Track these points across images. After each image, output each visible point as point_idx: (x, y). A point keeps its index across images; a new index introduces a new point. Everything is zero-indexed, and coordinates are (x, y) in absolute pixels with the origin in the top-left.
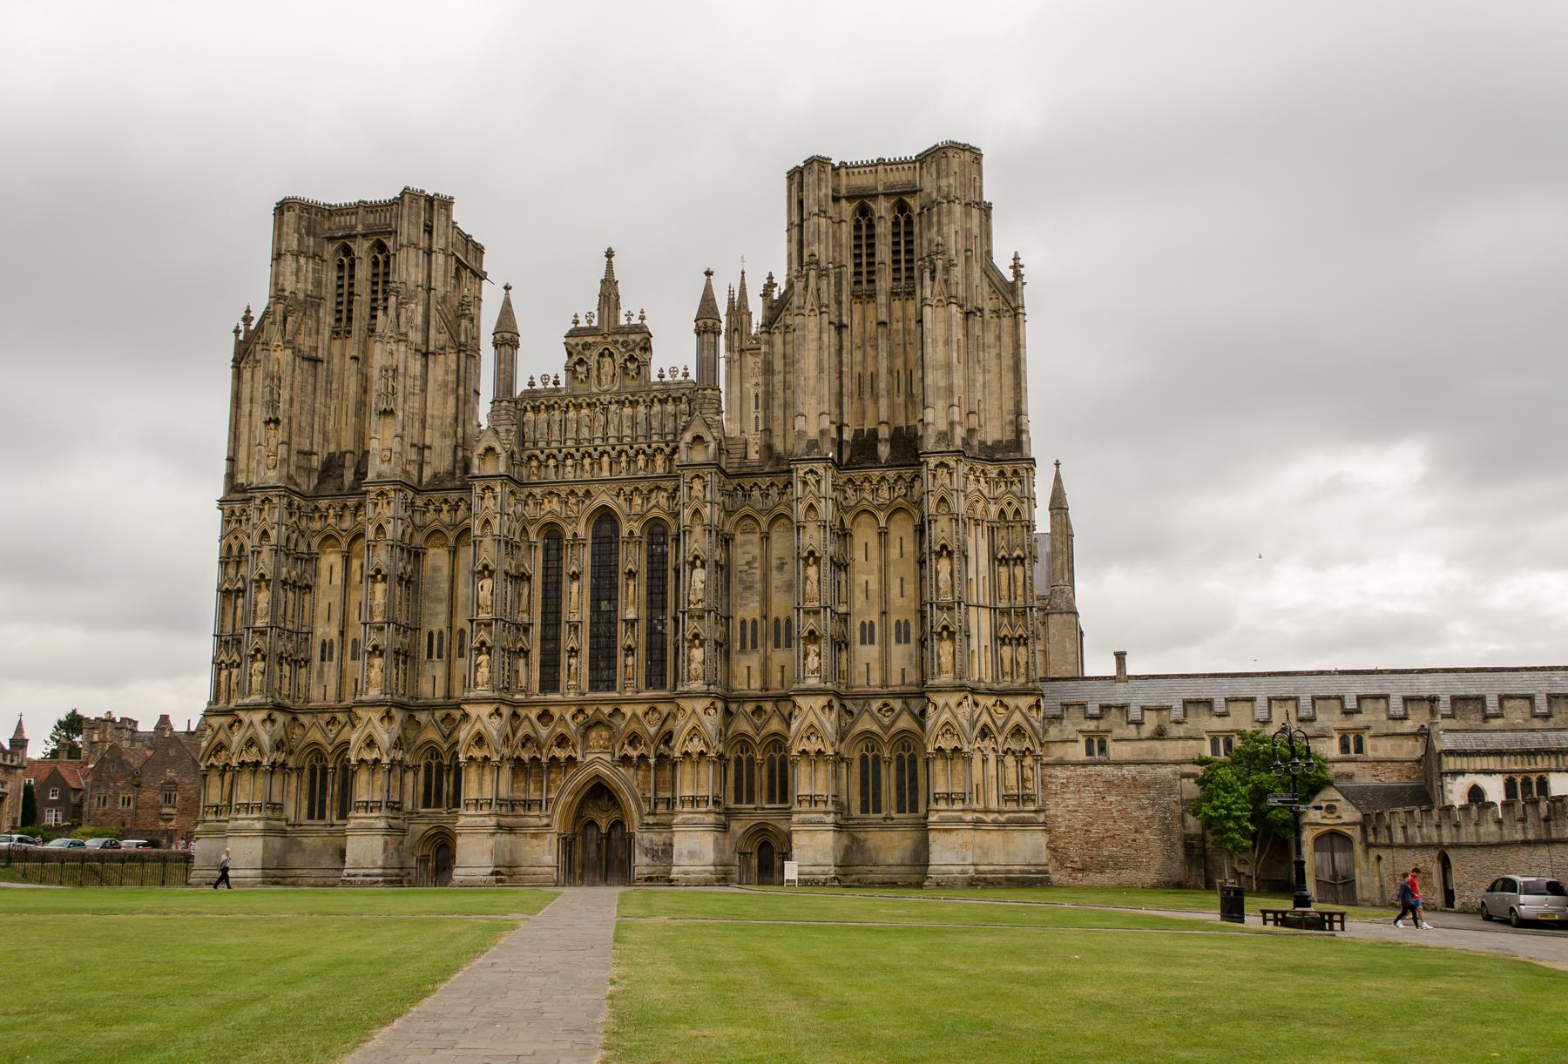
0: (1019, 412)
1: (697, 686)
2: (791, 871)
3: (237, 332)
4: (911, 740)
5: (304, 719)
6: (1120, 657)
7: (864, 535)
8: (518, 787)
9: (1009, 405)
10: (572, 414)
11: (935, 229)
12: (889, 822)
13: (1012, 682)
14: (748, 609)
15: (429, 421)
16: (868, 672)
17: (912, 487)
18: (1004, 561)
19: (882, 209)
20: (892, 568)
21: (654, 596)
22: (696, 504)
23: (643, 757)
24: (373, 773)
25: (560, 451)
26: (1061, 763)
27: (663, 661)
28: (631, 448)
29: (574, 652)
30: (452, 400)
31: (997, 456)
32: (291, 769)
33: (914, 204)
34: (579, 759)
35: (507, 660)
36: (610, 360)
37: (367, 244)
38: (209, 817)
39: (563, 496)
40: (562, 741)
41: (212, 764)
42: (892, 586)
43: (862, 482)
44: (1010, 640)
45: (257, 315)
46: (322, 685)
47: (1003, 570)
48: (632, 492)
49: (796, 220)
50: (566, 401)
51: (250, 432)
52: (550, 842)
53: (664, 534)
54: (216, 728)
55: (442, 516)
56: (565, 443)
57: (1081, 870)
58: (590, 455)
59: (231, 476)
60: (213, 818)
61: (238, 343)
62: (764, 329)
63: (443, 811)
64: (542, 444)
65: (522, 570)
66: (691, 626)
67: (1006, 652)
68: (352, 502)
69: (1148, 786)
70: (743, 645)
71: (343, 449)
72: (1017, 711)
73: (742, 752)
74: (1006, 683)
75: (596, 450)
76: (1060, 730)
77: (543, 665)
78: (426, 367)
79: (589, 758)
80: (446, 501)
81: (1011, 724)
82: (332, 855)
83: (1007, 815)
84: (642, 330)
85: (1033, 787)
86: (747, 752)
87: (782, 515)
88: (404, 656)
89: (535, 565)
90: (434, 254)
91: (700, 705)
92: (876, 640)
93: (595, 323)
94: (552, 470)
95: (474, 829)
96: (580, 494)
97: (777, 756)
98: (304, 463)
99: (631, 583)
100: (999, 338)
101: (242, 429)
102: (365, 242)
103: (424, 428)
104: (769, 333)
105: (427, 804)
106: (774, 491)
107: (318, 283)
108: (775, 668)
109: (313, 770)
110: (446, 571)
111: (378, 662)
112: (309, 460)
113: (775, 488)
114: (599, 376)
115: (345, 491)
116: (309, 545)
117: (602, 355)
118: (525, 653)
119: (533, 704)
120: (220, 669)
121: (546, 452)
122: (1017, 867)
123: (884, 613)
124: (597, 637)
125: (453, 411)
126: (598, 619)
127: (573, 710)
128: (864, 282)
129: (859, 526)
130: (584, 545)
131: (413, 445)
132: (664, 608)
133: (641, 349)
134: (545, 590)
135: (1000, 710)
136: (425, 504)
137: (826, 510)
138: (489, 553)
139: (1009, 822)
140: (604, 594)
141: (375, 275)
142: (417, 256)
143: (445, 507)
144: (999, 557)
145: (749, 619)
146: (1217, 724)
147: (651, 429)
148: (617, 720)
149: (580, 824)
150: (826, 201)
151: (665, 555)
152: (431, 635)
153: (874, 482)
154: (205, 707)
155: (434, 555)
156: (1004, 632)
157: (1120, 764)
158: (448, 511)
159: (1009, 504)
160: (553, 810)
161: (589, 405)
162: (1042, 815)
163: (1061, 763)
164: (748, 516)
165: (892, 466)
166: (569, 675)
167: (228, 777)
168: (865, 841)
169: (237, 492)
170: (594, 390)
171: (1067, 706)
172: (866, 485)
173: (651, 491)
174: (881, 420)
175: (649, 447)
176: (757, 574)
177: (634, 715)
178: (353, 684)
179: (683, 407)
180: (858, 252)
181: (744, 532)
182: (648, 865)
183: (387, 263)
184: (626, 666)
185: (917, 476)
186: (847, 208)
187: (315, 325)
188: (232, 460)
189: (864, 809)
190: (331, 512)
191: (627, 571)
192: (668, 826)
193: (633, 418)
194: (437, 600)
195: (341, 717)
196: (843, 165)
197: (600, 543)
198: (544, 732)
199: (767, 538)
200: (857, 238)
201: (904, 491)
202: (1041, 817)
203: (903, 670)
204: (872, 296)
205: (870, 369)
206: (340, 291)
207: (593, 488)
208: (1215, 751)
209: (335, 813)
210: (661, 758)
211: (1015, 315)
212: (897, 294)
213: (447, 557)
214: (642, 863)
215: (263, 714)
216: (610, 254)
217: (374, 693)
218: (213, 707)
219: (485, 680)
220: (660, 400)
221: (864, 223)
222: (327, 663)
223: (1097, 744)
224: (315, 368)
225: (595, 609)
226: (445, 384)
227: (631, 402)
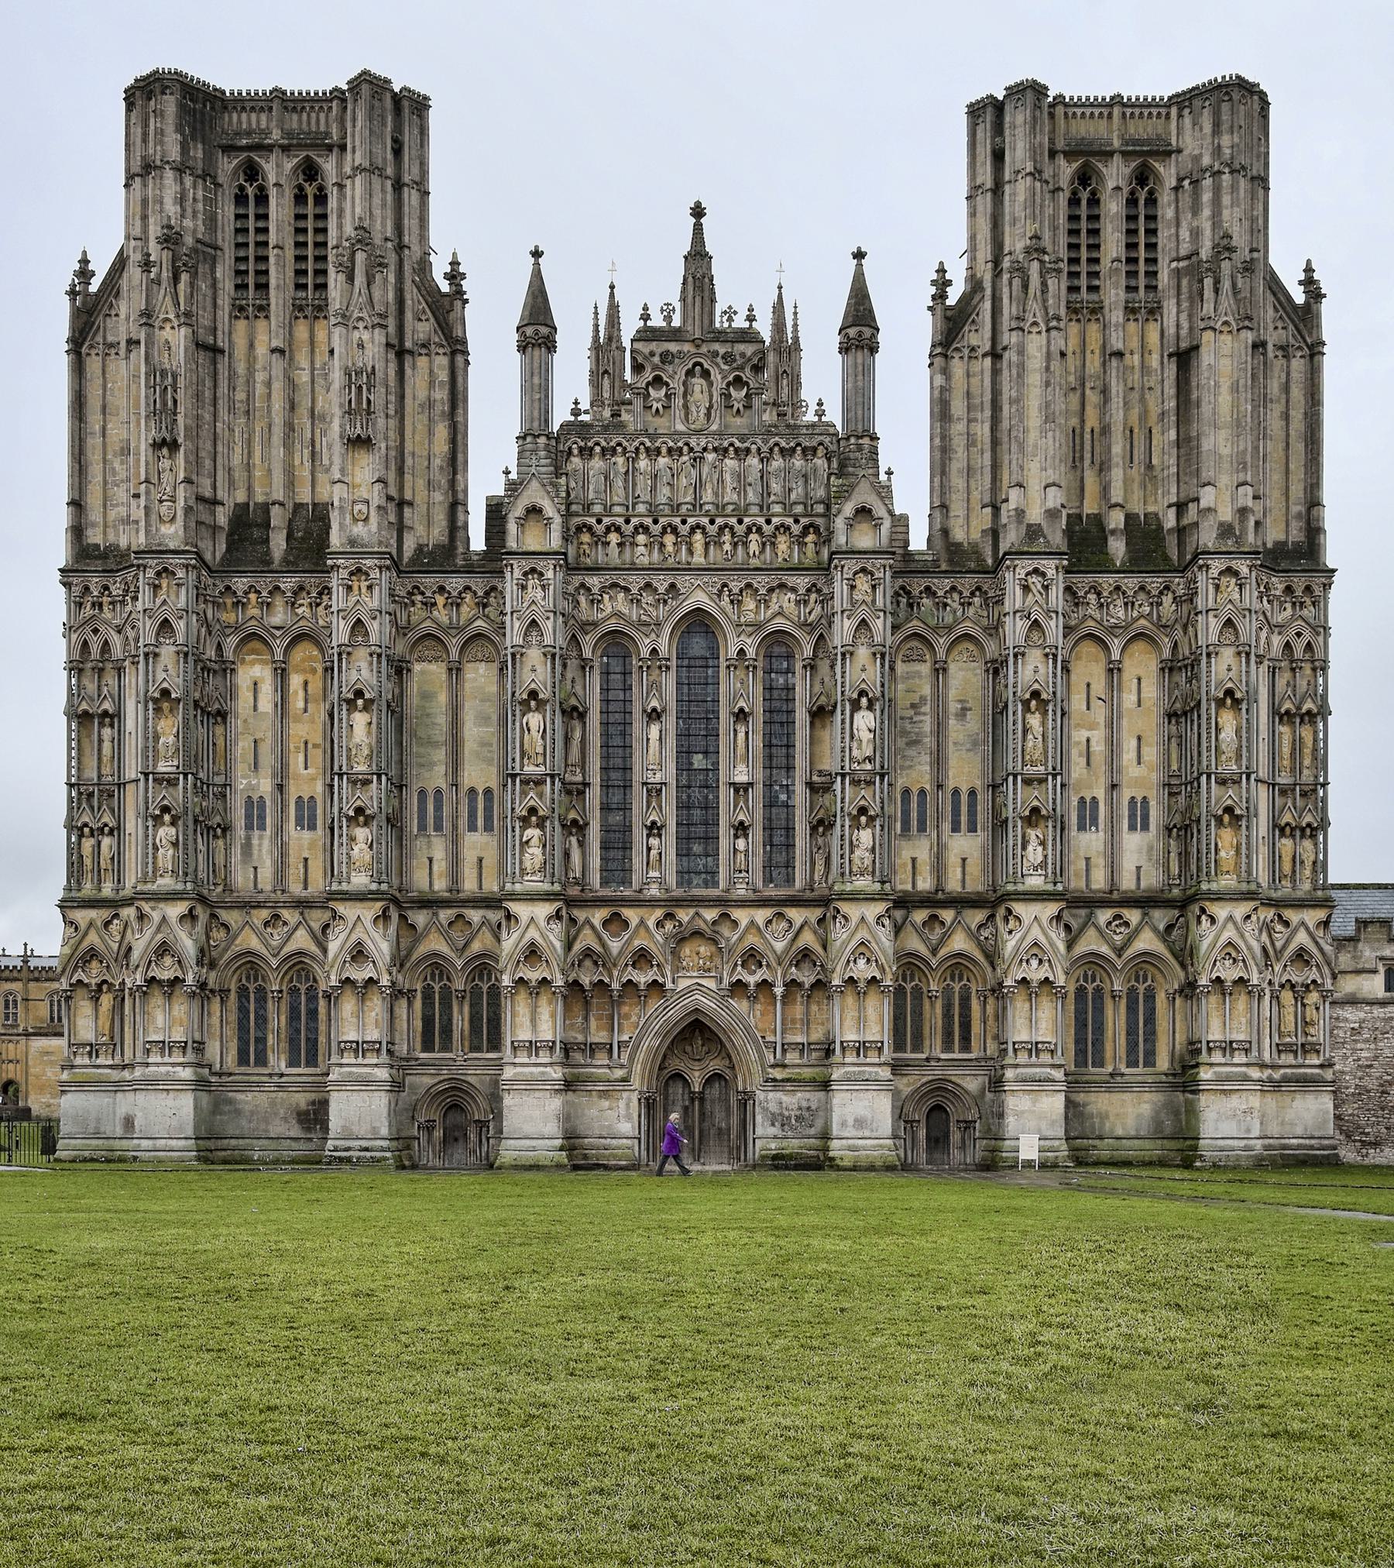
0: (1313, 502)
3: (72, 293)
4: (1152, 969)
5: (225, 915)
7: (1089, 669)
8: (572, 1025)
9: (1297, 490)
10: (643, 463)
11: (1206, 212)
12: (1119, 1079)
13: (1294, 888)
14: (918, 774)
15: (409, 461)
16: (1087, 870)
17: (1159, 604)
18: (1286, 717)
19: (1115, 174)
20: (1125, 722)
21: (774, 750)
23: (765, 985)
25: (627, 522)
26: (1353, 1001)
27: (790, 846)
28: (740, 522)
29: (654, 829)
30: (442, 431)
31: (1283, 566)
32: (212, 991)
33: (1168, 173)
34: (669, 985)
36: (702, 381)
37: (289, 165)
38: (78, 1061)
39: (634, 591)
40: (642, 958)
41: (80, 981)
42: (1125, 747)
43: (1086, 593)
44: (1292, 829)
47: (1285, 730)
48: (741, 591)
50: (636, 443)
51: (105, 461)
52: (628, 1105)
53: (790, 657)
54: (83, 926)
56: (634, 508)
57: (1371, 1144)
58: (675, 531)
59: (77, 531)
60: (87, 1061)
62: (939, 350)
63: (457, 1054)
64: (597, 509)
65: (573, 702)
67: (1286, 845)
72: (1302, 929)
73: (904, 980)
74: (1285, 890)
75: (684, 522)
76: (1354, 957)
77: (605, 847)
78: (401, 373)
79: (683, 984)
80: (442, 589)
81: (1293, 947)
82: (285, 1119)
83: (1282, 1071)
85: (1318, 1034)
86: (912, 980)
87: (967, 637)
90: (406, 189)
92: (1101, 826)
93: (676, 322)
96: (662, 590)
97: (957, 987)
98: (205, 517)
99: (741, 729)
100: (1286, 388)
101: (89, 454)
102: (285, 159)
103: (401, 471)
104: (946, 356)
105: (428, 1046)
106: (954, 602)
107: (211, 221)
108: (953, 860)
109: (243, 992)
110: (443, 698)
112: (213, 513)
113: (956, 596)
114: (686, 407)
115: (275, 566)
116: (219, 647)
117: (690, 373)
118: (578, 828)
120: (81, 836)
121: (606, 520)
122: (1294, 1141)
123: (1114, 786)
124: (688, 808)
125: (446, 448)
126: (689, 780)
127: (659, 913)
128: (1084, 289)
129: (1078, 658)
130: (668, 668)
132: (790, 768)
134: (606, 735)
135: (1279, 927)
136: (409, 593)
139: (1286, 1080)
141: (300, 217)
142: (383, 191)
143: (440, 600)
144: (1283, 710)
145: (915, 791)
147: (769, 494)
148: (725, 930)
150: (1042, 154)
151: (790, 689)
152: (422, 793)
153: (1105, 594)
154: (61, 895)
155: (422, 672)
156: (1287, 818)
159: (1299, 635)
160: (631, 1059)
161: (670, 450)
162: (1331, 1071)
163: (1353, 1001)
164: (916, 636)
165: (1132, 572)
167: (106, 1000)
168: (1085, 1105)
169: (96, 558)
170: (680, 427)
171: (1362, 924)
172: (1092, 597)
173: (771, 590)
174: (1113, 501)
175: (768, 522)
176: (927, 724)
177: (752, 923)
178: (301, 866)
179: (820, 462)
180: (1074, 241)
181: (907, 660)
182: (775, 1137)
185: (1167, 588)
186: (1066, 170)
187: (209, 293)
188: (77, 504)
190: (253, 596)
191: (736, 710)
194: (432, 743)
195: (286, 914)
196: (1059, 99)
197: (688, 667)
198: (615, 945)
199: (945, 670)
200: (1073, 218)
201: (1147, 609)
202: (1329, 1075)
203: (1138, 868)
204: (1097, 310)
205: (1092, 420)
206: (240, 240)
207: (683, 582)
209: (283, 1057)
210: (792, 985)
211: (1312, 356)
212: (1134, 311)
213: (444, 677)
214: (766, 1137)
216: (698, 212)
218: (74, 894)
220: (782, 450)
221: (1084, 196)
222: (256, 832)
224: (214, 363)
225: (684, 766)
226: (430, 403)
227: (737, 450)
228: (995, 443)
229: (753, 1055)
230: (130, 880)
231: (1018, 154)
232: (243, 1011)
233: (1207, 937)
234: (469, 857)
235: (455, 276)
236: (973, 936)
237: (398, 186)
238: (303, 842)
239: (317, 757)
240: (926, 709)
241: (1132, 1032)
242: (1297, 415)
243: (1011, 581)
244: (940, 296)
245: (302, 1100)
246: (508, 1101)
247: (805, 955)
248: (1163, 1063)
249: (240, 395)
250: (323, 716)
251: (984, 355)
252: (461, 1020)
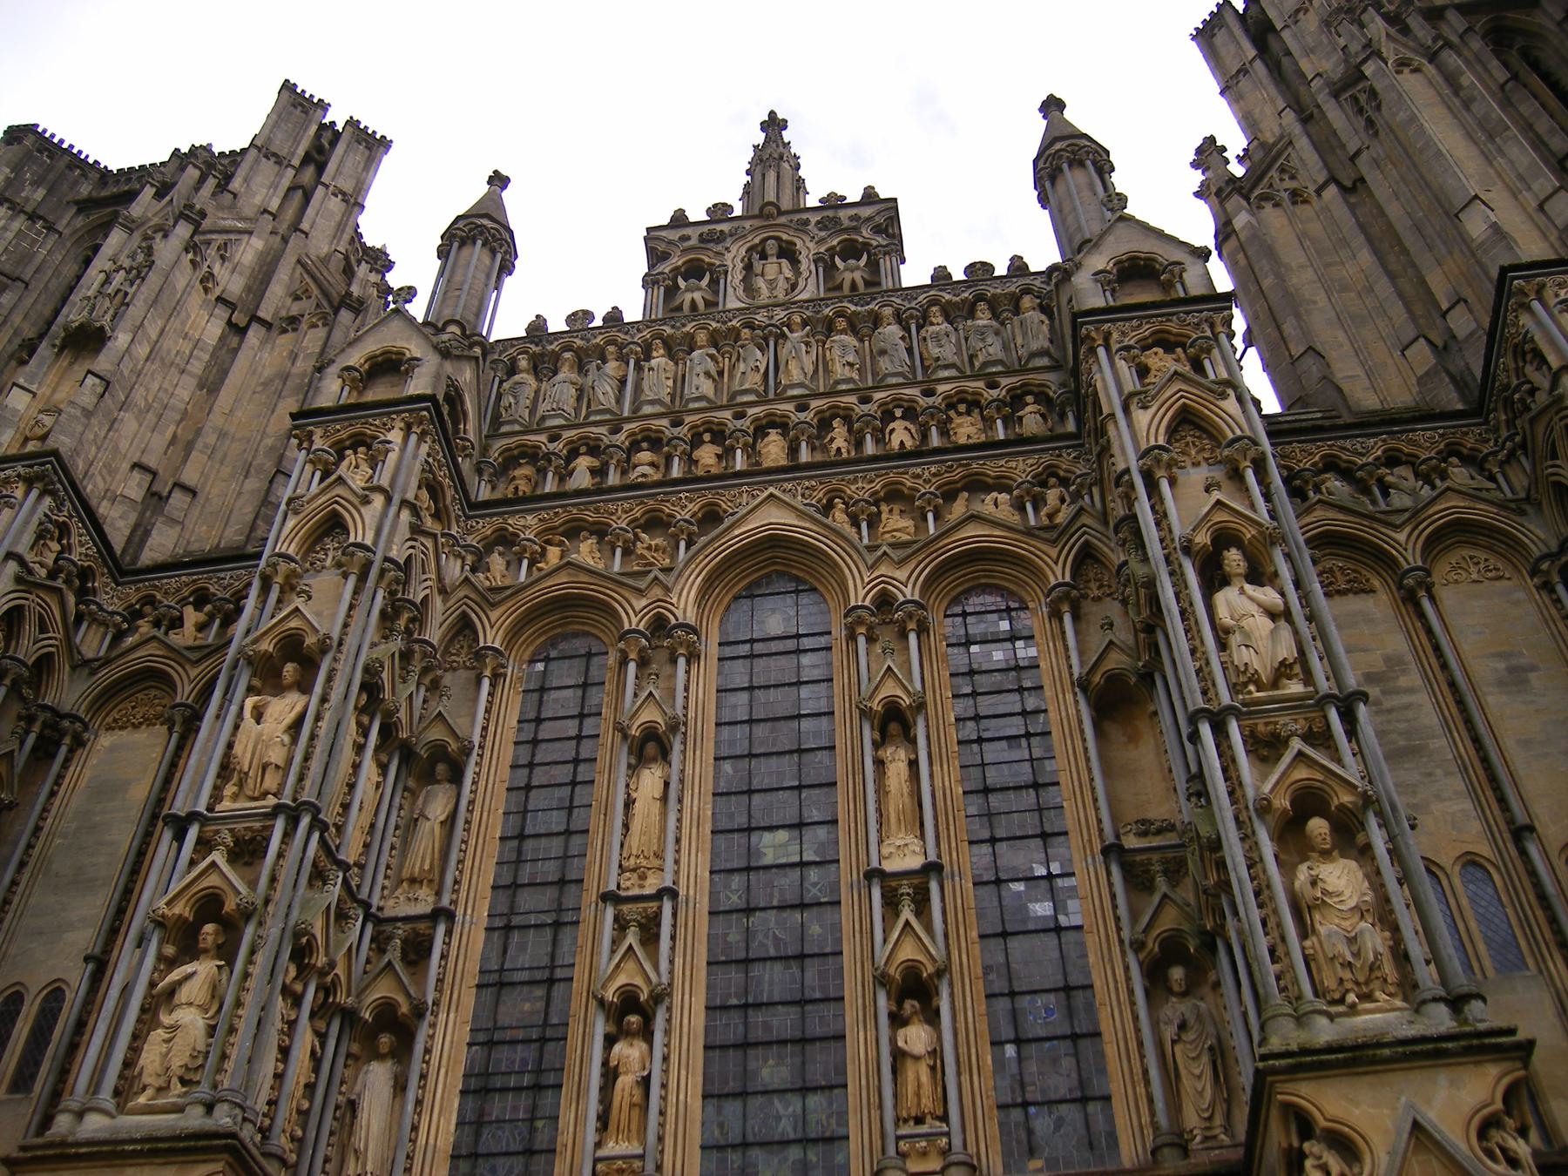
10: (659, 360)
21: (995, 800)
22: (1174, 395)
27: (1083, 1038)
35: (304, 1040)
36: (784, 262)
55: (175, 638)
65: (436, 733)
77: (478, 1087)
94: (582, 477)
130: (693, 657)
131: (137, 466)
133: (878, 230)
155: (112, 749)
158: (201, 627)
166: (604, 1120)
173: (950, 496)
184: (899, 1056)
197: (752, 656)
219: (178, 1061)
240: (1413, 678)
251: (1319, 191)
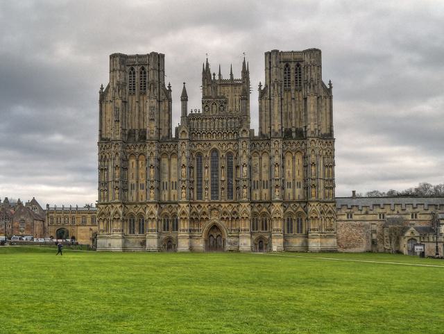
0: (331, 126)
1: (245, 199)
2: (275, 248)
3: (100, 92)
6: (354, 192)
7: (289, 158)
9: (328, 123)
19: (293, 65)
23: (227, 218)
24: (152, 221)
26: (341, 221)
29: (207, 189)
30: (167, 115)
33: (302, 65)
37: (139, 68)
40: (204, 213)
45: (105, 87)
46: (132, 197)
49: (268, 67)
59: (100, 135)
61: (100, 96)
66: (242, 183)
67: (327, 191)
68: (139, 144)
69: (363, 226)
70: (254, 188)
71: (134, 128)
74: (327, 200)
77: (197, 192)
84: (223, 97)
85: (334, 227)
88: (158, 189)
89: (195, 164)
91: (246, 204)
95: (183, 237)
105: (164, 230)
107: (125, 79)
108: (263, 194)
109: (130, 220)
110: (167, 165)
111: (152, 191)
118: (192, 189)
119: (196, 203)
123: (294, 180)
132: (232, 177)
137: (280, 151)
138: (184, 161)
140: (215, 173)
146: (381, 211)
149: (209, 235)
152: (163, 183)
157: (356, 221)
163: (341, 221)
167: (105, 222)
171: (342, 205)
176: (258, 168)
183: (145, 73)
185: (303, 142)
186: (283, 65)
188: (100, 131)
189: (288, 233)
192: (238, 237)
193: (222, 123)
196: (282, 52)
198: (199, 211)
204: (290, 90)
207: (212, 143)
208: (380, 218)
210: (233, 218)
214: (228, 247)
215: (120, 205)
217: (152, 200)
221: (287, 69)
223: (350, 215)
225: (212, 177)
228: (270, 116)
229: (225, 231)
230: (110, 200)
231: (273, 63)
232: (130, 223)
233: (310, 209)
234: (172, 195)
235: (169, 87)
236: (267, 209)
237: (159, 71)
238: (141, 191)
239: (144, 176)
241: (298, 226)
242: (328, 109)
243: (272, 143)
244: (260, 89)
245: (141, 240)
246: (179, 240)
247: (235, 212)
248: (304, 233)
249: (130, 109)
250: (145, 168)
252: (171, 225)
